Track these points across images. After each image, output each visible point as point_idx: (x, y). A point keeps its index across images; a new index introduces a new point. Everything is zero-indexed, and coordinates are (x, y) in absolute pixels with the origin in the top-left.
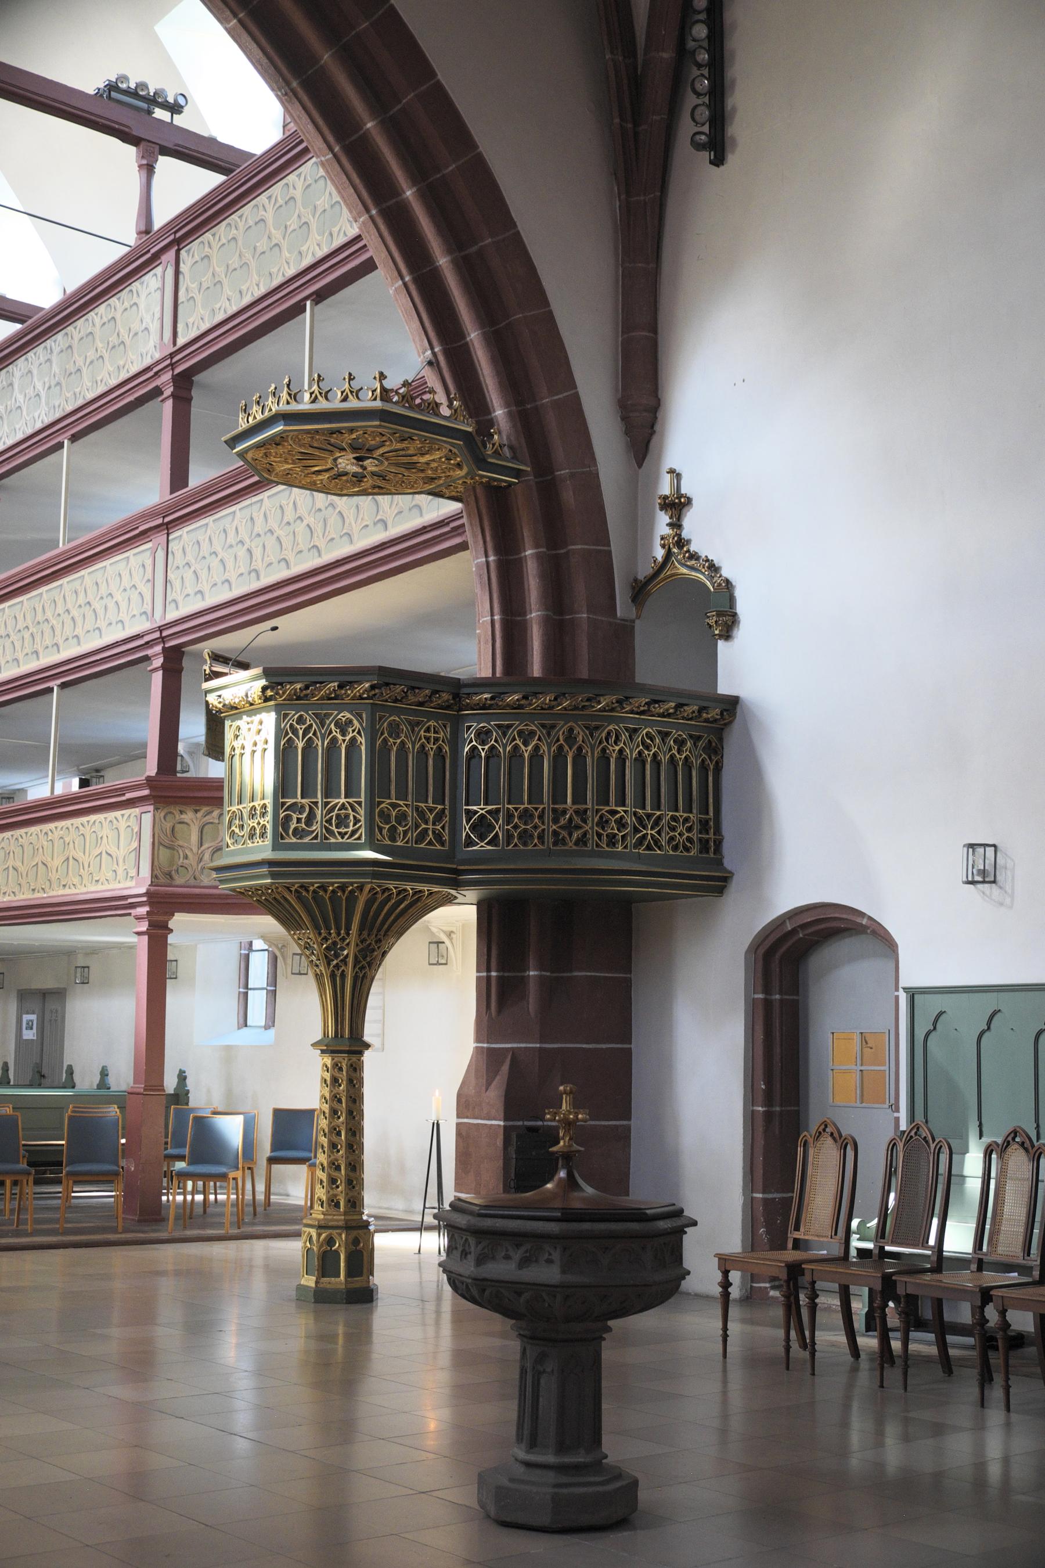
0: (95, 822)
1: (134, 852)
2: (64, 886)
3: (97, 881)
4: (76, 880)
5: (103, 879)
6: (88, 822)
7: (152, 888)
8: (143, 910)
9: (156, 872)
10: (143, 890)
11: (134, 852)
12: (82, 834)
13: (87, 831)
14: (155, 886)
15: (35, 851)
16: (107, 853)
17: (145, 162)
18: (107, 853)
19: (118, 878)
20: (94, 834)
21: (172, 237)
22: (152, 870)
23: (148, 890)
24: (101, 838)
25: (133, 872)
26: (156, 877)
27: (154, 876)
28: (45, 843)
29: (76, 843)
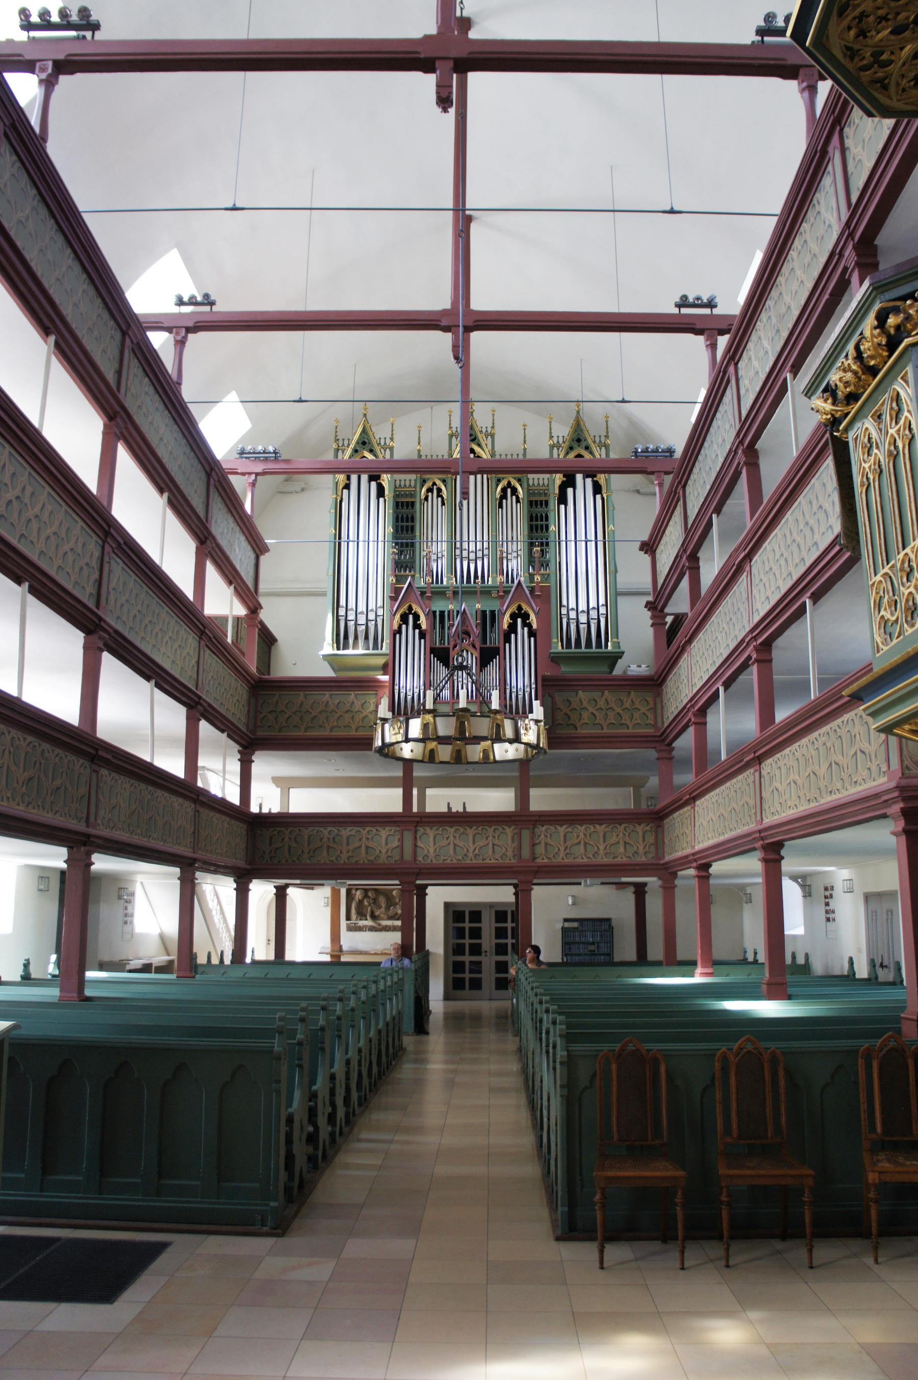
0: (848, 721)
1: (883, 745)
2: (831, 792)
3: (856, 782)
4: (839, 785)
5: (860, 780)
6: (843, 722)
7: (904, 782)
8: (897, 808)
9: (906, 763)
10: (893, 784)
11: (883, 745)
12: (840, 737)
13: (843, 732)
14: (907, 778)
15: (807, 761)
16: (861, 751)
17: (805, 84)
18: (861, 751)
19: (873, 775)
20: (849, 734)
21: (832, 118)
22: (902, 761)
23: (898, 783)
24: (855, 736)
25: (884, 768)
26: (907, 768)
27: (904, 768)
28: (813, 752)
29: (836, 745)
